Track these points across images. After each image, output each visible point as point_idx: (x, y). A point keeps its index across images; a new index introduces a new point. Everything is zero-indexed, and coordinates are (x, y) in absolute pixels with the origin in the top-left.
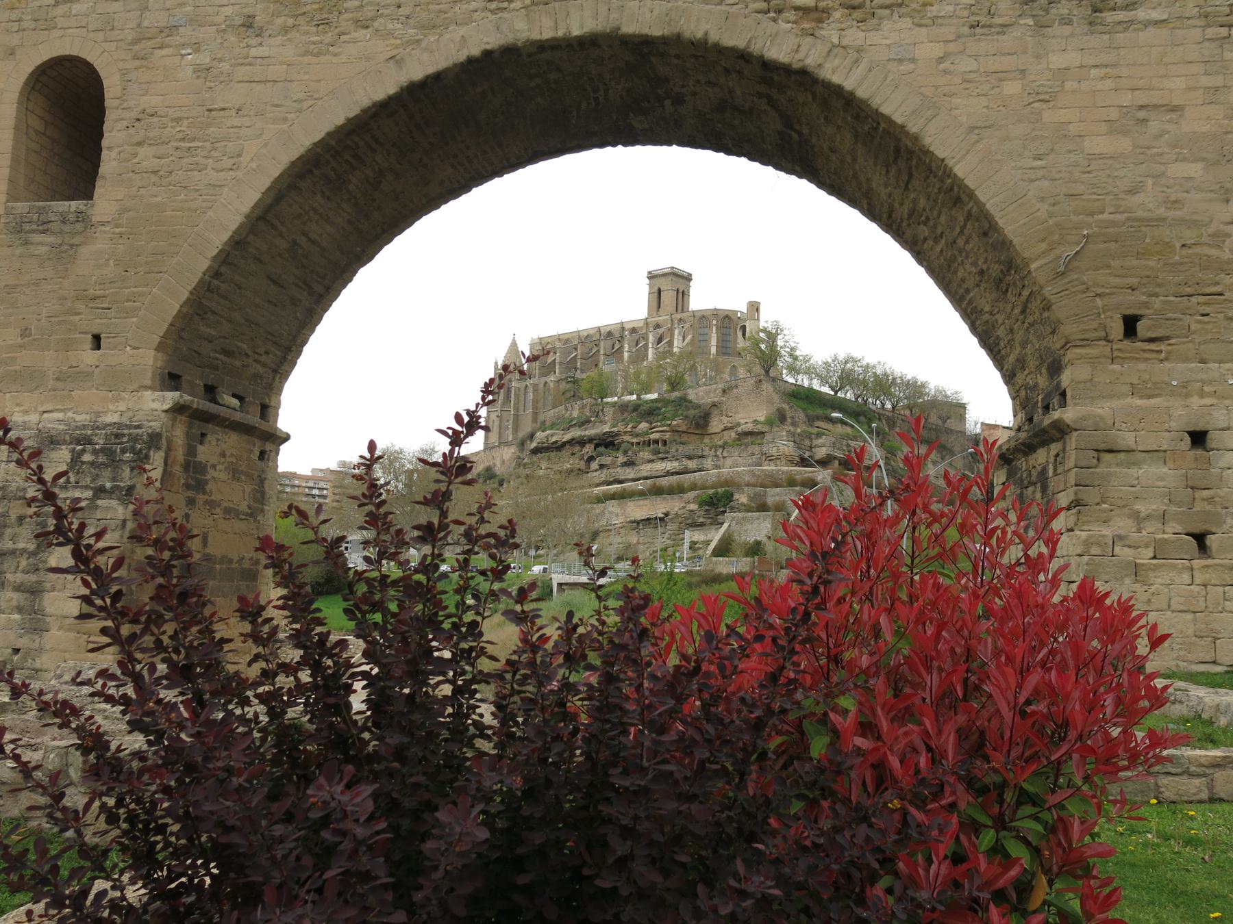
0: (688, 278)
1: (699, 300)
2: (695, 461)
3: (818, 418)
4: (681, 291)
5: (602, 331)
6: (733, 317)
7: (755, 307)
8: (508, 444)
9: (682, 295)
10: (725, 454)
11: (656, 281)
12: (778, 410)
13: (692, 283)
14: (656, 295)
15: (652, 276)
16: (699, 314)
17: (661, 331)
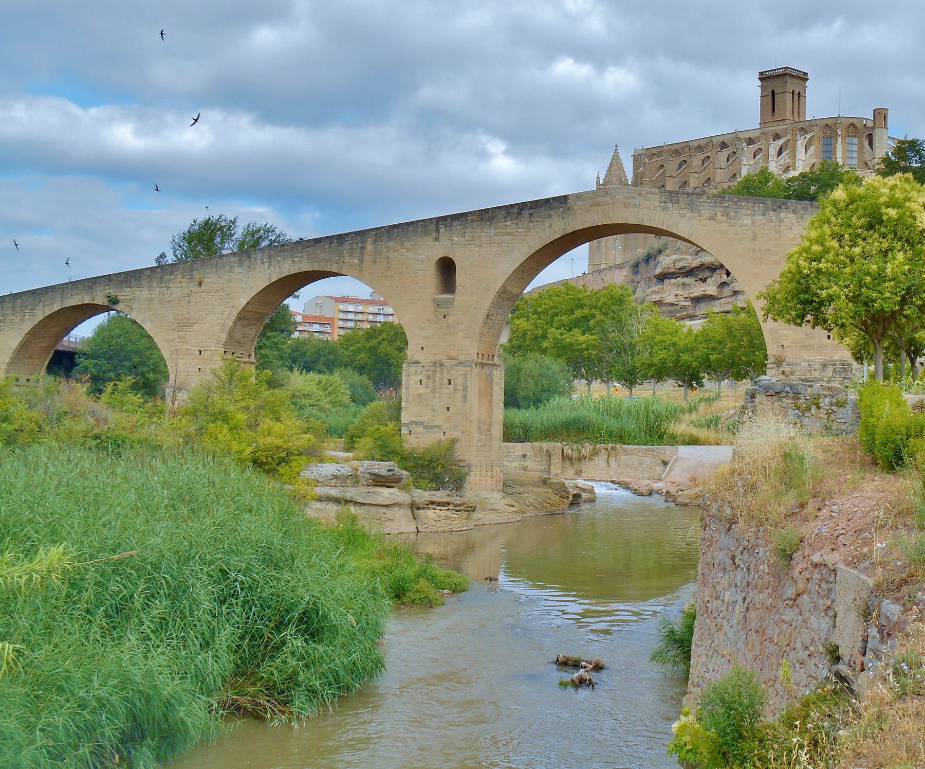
5: (714, 140)
8: (620, 267)
9: (799, 97)
11: (766, 83)
13: (808, 83)
14: (770, 98)
15: (765, 78)
17: (780, 142)
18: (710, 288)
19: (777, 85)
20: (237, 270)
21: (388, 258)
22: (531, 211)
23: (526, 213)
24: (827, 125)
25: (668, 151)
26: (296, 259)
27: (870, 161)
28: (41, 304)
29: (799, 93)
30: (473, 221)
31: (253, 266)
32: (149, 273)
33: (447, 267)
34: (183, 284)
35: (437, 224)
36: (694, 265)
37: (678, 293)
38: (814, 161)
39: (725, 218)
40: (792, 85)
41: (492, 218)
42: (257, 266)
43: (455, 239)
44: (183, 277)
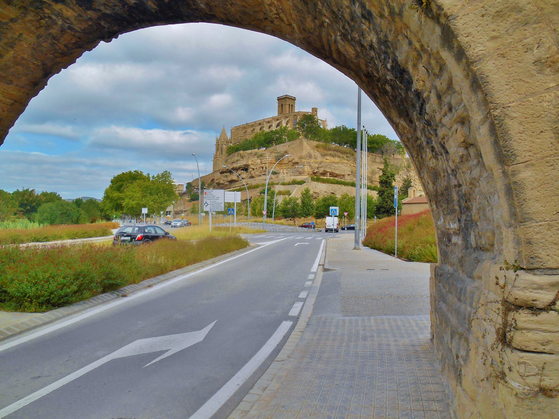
0: (294, 99)
1: (299, 108)
2: (275, 175)
3: (326, 155)
4: (291, 105)
5: (257, 122)
9: (292, 106)
10: (287, 172)
15: (279, 99)
18: (234, 177)
19: (283, 102)
25: (242, 127)
29: (292, 105)
37: (224, 179)
40: (289, 102)
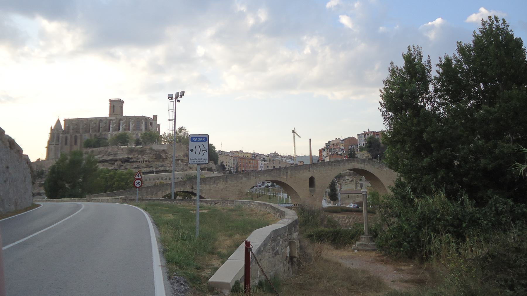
6: (147, 119)
7: (155, 117)
9: (121, 108)
12: (186, 153)
16: (137, 117)
20: (244, 179)
21: (295, 176)
22: (335, 164)
23: (333, 164)
24: (138, 118)
26: (265, 176)
27: (151, 130)
28: (161, 191)
30: (319, 166)
31: (250, 178)
32: (209, 179)
33: (312, 181)
34: (223, 184)
35: (309, 166)
36: (108, 159)
38: (134, 128)
39: (380, 168)
41: (325, 165)
42: (251, 178)
43: (315, 171)
44: (223, 181)
